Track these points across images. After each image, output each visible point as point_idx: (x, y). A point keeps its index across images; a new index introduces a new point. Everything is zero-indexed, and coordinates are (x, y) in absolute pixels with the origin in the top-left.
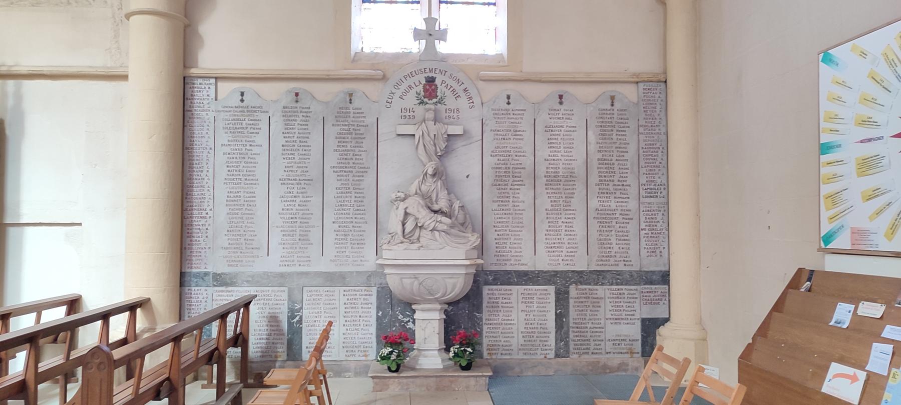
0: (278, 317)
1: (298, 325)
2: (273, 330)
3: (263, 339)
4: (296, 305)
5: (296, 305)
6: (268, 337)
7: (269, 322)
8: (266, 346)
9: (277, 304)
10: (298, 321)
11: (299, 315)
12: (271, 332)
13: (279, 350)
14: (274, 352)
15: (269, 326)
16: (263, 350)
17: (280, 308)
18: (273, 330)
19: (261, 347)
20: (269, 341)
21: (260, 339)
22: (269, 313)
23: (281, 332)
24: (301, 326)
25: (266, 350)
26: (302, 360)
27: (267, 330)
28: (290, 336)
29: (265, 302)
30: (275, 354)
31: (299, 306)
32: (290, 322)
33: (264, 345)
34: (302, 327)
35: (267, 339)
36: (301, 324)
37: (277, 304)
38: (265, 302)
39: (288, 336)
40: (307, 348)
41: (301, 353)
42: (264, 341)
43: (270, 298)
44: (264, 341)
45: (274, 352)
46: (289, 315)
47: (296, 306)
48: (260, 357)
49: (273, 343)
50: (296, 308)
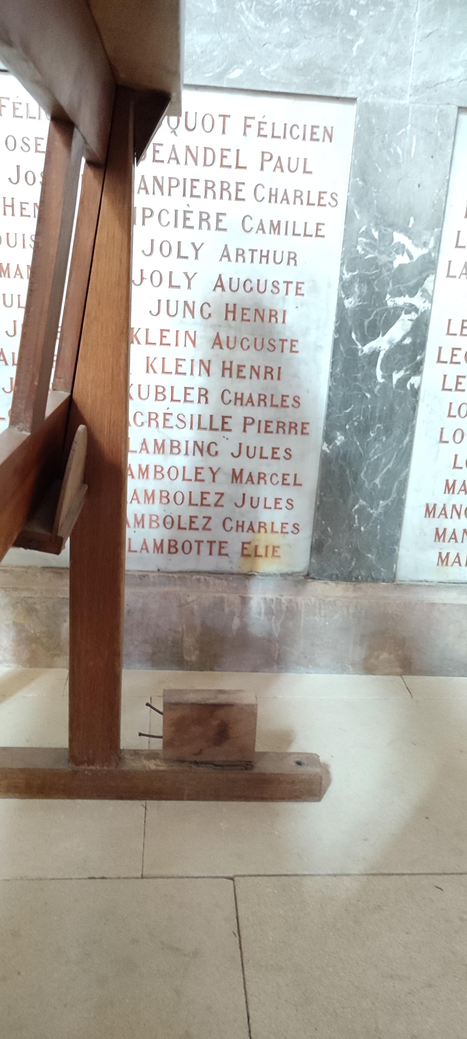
0: (273, 314)
1: (396, 376)
2: (239, 399)
3: (175, 447)
4: (399, 237)
5: (399, 237)
6: (206, 437)
7: (217, 342)
8: (197, 488)
9: (275, 228)
10: (398, 347)
11: (412, 308)
12: (230, 410)
13: (265, 516)
14: (240, 526)
15: (216, 369)
16: (174, 510)
17: (292, 258)
18: (239, 399)
19: (166, 497)
20: (214, 462)
21: (160, 448)
22: (220, 284)
23: (289, 415)
24: (414, 380)
25: (193, 511)
26: (392, 579)
27: (204, 394)
28: (340, 439)
29: (197, 206)
30: (246, 536)
31: (418, 252)
32: (353, 352)
33: (180, 486)
34: (415, 392)
35: (200, 448)
36: (417, 369)
37: (275, 228)
38: (197, 206)
39: (328, 438)
40: (430, 511)
41: (396, 541)
42: (180, 461)
43: (232, 176)
44: (180, 461)
45: (240, 526)
46: (350, 303)
47: (401, 249)
48: (159, 548)
49: (236, 477)
50: (400, 260)
